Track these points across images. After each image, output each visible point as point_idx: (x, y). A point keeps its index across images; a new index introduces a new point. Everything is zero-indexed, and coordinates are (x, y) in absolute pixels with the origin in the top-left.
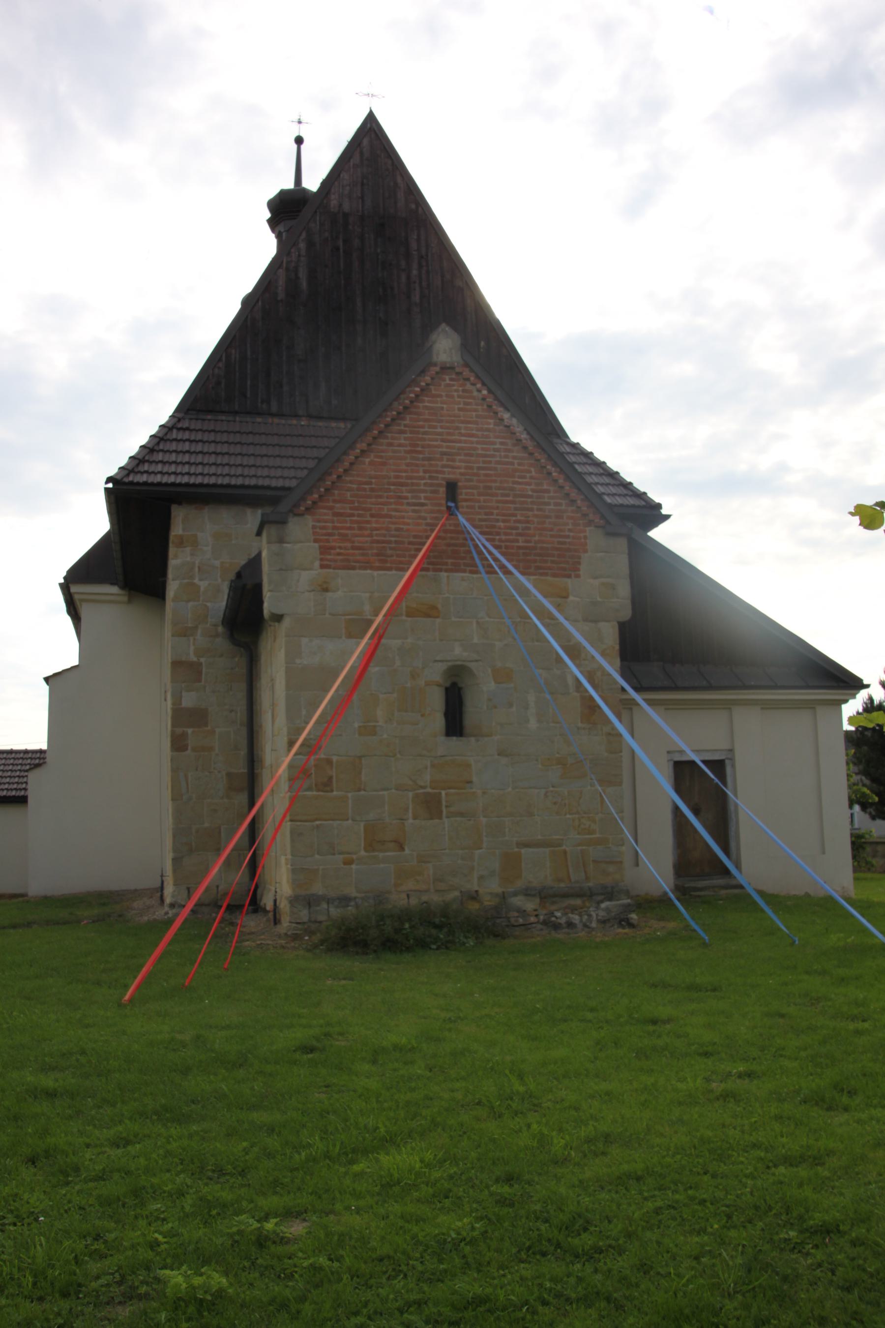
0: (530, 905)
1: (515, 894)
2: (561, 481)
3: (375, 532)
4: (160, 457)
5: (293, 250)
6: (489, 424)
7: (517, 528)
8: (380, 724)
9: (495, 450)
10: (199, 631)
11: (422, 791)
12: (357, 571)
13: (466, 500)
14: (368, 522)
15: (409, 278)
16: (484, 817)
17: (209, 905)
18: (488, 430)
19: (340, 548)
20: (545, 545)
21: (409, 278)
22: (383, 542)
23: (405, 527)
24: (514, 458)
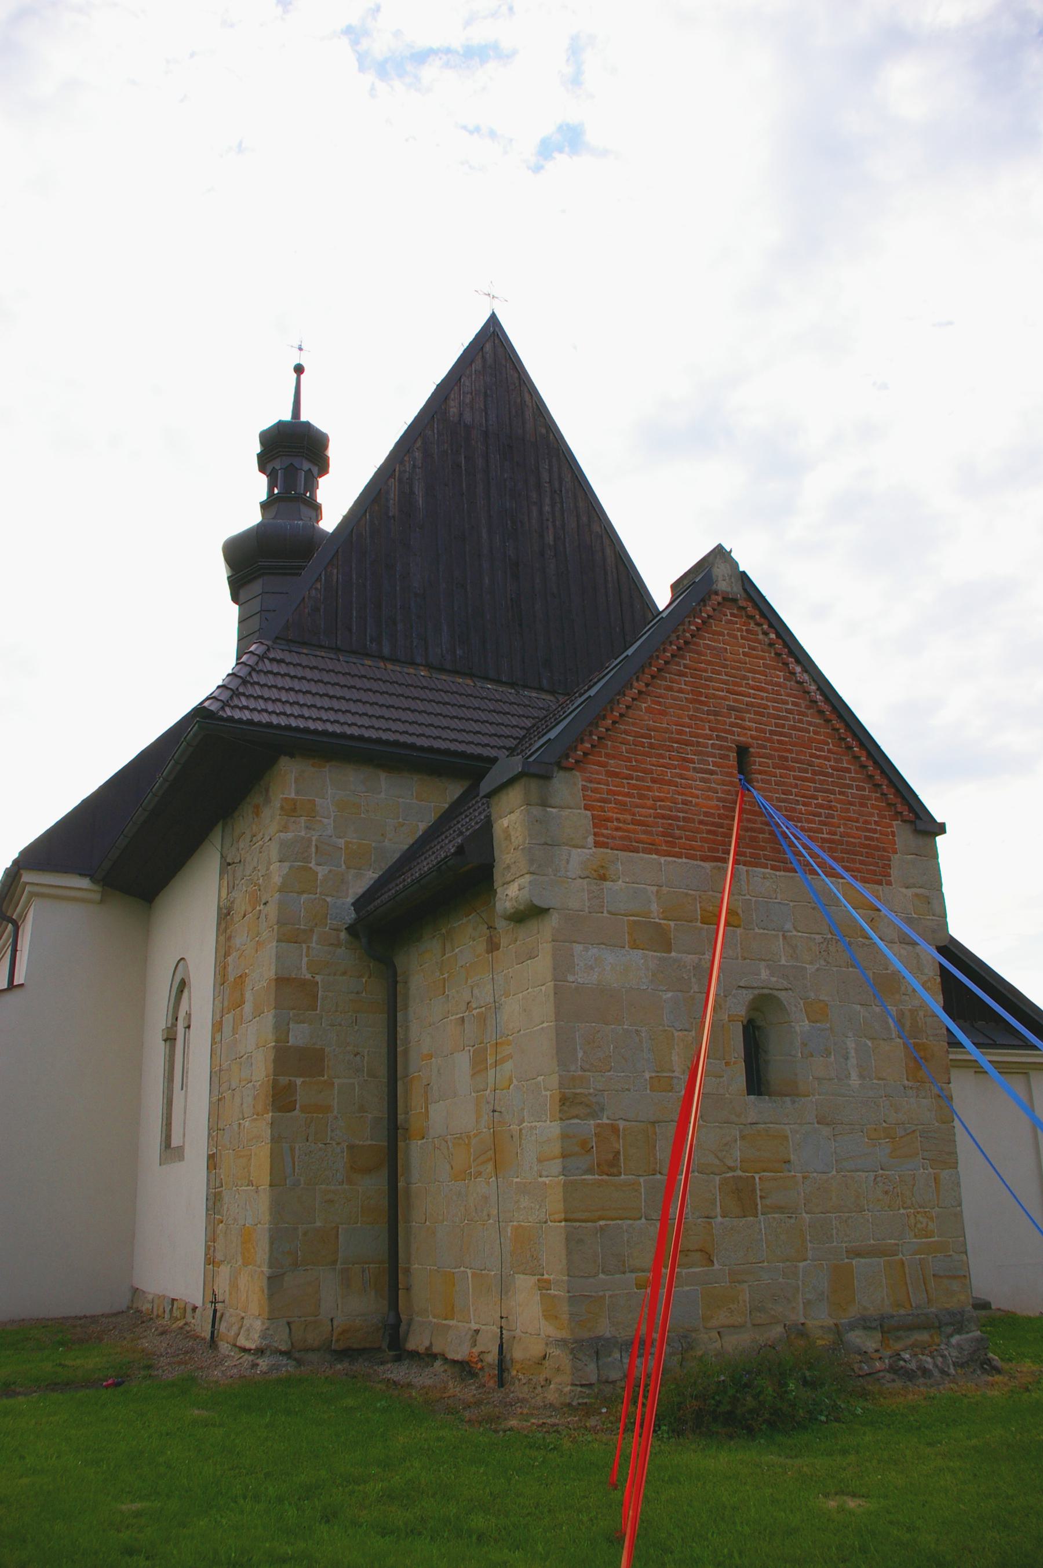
0: (870, 1342)
1: (852, 1327)
2: (863, 759)
3: (659, 803)
5: (406, 458)
6: (778, 677)
7: (819, 815)
8: (676, 1074)
9: (788, 711)
10: (315, 938)
11: (730, 1174)
12: (641, 854)
13: (760, 772)
14: (649, 789)
15: (541, 512)
16: (807, 1213)
17: (318, 1350)
18: (778, 685)
19: (618, 820)
20: (852, 840)
21: (541, 512)
22: (670, 818)
23: (694, 800)
24: (810, 724)
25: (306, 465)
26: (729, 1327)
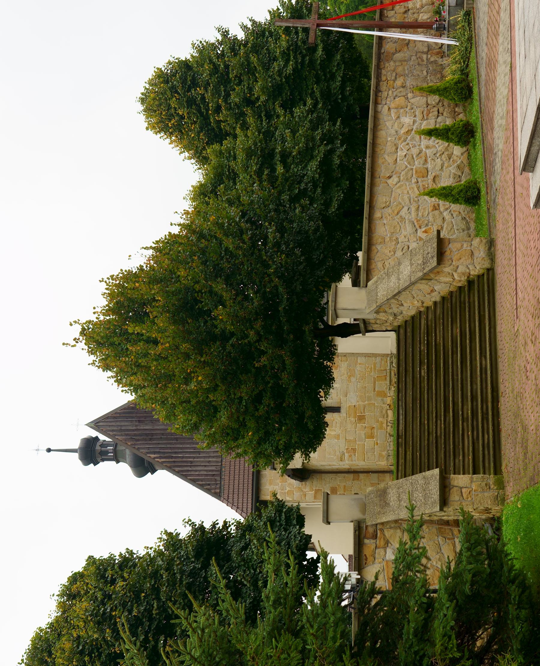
4: (240, 504)
25: (98, 448)
26: (478, 73)
